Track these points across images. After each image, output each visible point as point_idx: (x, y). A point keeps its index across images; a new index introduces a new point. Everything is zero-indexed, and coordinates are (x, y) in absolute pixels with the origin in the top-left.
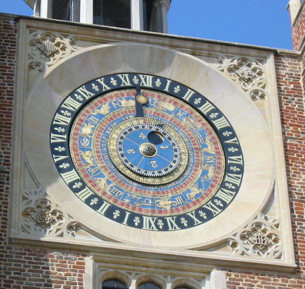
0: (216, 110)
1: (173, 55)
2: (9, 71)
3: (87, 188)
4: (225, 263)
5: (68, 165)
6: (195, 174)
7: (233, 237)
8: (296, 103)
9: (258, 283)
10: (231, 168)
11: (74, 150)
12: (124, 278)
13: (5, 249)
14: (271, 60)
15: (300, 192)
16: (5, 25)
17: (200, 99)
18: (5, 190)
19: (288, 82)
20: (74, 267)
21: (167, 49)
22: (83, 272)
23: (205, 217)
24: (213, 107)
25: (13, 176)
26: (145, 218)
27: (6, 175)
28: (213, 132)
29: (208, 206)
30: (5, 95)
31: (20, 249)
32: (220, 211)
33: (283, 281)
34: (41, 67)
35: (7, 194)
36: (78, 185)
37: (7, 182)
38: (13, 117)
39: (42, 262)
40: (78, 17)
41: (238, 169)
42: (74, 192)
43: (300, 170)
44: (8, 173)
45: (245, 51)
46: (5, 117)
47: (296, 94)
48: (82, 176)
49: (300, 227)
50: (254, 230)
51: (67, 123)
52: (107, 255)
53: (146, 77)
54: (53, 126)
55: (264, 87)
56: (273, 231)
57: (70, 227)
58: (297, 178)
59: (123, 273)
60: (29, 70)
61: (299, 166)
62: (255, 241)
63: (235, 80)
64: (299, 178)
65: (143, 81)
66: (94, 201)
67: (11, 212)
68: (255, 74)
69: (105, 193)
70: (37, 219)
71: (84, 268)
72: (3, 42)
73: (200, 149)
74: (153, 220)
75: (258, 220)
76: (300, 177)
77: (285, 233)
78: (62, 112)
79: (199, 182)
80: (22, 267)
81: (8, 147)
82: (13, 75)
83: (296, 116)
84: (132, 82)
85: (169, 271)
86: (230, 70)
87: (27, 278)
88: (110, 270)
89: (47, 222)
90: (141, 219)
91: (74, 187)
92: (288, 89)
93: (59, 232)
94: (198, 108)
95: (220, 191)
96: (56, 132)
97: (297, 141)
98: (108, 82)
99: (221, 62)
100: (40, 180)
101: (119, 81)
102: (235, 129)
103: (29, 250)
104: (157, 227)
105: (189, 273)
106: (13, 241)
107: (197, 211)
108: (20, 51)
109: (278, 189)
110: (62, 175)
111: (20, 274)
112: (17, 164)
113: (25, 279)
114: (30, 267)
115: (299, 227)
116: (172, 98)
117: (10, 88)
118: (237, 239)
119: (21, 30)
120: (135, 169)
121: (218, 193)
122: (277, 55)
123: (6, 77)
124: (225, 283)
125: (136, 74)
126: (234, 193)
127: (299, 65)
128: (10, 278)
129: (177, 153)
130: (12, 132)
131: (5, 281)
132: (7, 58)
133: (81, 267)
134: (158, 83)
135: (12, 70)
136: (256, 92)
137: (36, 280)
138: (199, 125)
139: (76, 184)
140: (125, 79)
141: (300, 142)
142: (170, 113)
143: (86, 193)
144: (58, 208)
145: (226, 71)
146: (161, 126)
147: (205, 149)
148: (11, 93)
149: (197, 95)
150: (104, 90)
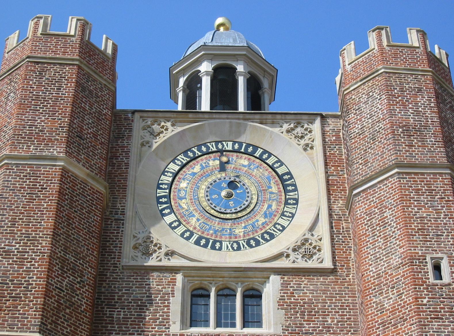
0: (279, 161)
1: (246, 125)
3: (182, 225)
4: (280, 270)
5: (169, 211)
6: (262, 208)
7: (287, 251)
8: (337, 150)
9: (305, 282)
10: (289, 201)
11: (174, 199)
12: (207, 287)
13: (119, 274)
14: (318, 121)
17: (267, 154)
21: (241, 121)
22: (175, 285)
23: (268, 238)
26: (223, 243)
27: (122, 222)
28: (277, 177)
31: (131, 273)
33: (323, 279)
34: (150, 144)
40: (200, 108)
41: (294, 202)
42: (173, 229)
43: (339, 197)
44: (123, 220)
45: (299, 117)
48: (179, 217)
50: (303, 244)
52: (193, 272)
54: (159, 184)
55: (313, 141)
56: (317, 244)
57: (167, 254)
58: (337, 203)
59: (232, 285)
65: (226, 146)
66: (187, 234)
68: (307, 132)
69: (195, 228)
71: (176, 282)
73: (267, 190)
74: (230, 243)
75: (306, 237)
76: (339, 203)
77: (326, 245)
78: (166, 174)
79: (265, 213)
80: (131, 285)
81: (124, 202)
84: (217, 147)
85: (239, 279)
86: (288, 131)
87: (134, 292)
88: (196, 282)
91: (173, 225)
92: (331, 140)
93: (159, 258)
96: (162, 189)
98: (200, 150)
99: (281, 127)
101: (208, 148)
102: (292, 173)
103: (136, 273)
104: (233, 248)
105: (254, 279)
106: (125, 267)
107: (263, 234)
108: (134, 134)
109: (321, 213)
111: (129, 290)
112: (129, 213)
113: (133, 294)
114: (136, 284)
116: (246, 156)
118: (290, 252)
119: (135, 120)
120: (217, 209)
122: (323, 117)
123: (124, 153)
124: (280, 284)
125: (221, 142)
126: (290, 219)
127: (340, 122)
128: (122, 293)
129: (249, 195)
131: (118, 296)
134: (236, 146)
136: (307, 145)
137: (140, 294)
138: (266, 174)
140: (212, 146)
141: (339, 178)
142: (245, 166)
143: (182, 229)
144: (159, 242)
145: (285, 132)
146: (238, 176)
148: (127, 165)
149: (265, 152)
150: (197, 155)
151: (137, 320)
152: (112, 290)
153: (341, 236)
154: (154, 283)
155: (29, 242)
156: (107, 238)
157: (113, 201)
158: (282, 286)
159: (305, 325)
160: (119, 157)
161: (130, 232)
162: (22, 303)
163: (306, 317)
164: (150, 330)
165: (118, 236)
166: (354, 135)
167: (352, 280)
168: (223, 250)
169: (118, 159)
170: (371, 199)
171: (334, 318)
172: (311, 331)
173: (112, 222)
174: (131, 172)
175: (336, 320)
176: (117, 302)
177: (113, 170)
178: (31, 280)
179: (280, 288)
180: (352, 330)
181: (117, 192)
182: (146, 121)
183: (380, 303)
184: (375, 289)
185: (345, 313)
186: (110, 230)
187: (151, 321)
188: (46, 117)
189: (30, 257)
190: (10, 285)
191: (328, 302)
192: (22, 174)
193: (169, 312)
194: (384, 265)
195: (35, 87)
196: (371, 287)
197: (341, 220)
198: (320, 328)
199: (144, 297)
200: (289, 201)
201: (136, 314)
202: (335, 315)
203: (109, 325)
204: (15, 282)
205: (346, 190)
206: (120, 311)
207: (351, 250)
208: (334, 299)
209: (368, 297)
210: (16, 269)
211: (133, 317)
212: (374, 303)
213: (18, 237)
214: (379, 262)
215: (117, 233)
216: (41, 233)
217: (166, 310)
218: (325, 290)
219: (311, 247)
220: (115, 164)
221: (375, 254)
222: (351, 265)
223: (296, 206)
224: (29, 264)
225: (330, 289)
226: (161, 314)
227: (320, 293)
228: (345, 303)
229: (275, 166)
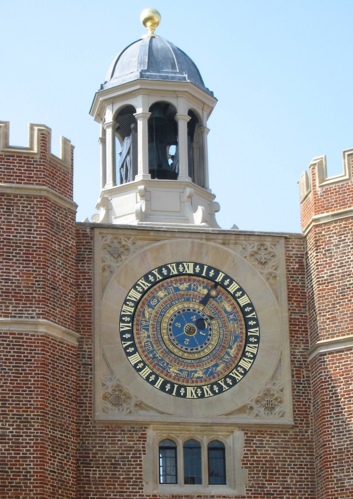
5: (133, 349)
7: (249, 403)
8: (300, 280)
9: (267, 439)
10: (251, 339)
16: (83, 234)
20: (139, 437)
21: (204, 241)
22: (145, 441)
25: (94, 368)
27: (90, 367)
30: (86, 298)
31: (102, 427)
36: (140, 366)
39: (117, 435)
43: (300, 340)
44: (91, 365)
45: (263, 238)
46: (87, 317)
52: (162, 426)
60: (103, 272)
66: (152, 378)
67: (94, 398)
71: (146, 438)
72: (83, 250)
74: (194, 389)
75: (268, 386)
76: (300, 346)
80: (104, 441)
81: (90, 343)
84: (178, 270)
85: (205, 433)
87: (108, 449)
88: (164, 435)
90: (186, 390)
92: (294, 268)
93: (129, 410)
95: (242, 360)
96: (124, 322)
98: (160, 272)
100: (113, 369)
101: (169, 271)
103: (108, 427)
104: (197, 395)
105: (219, 433)
111: (102, 447)
112: (98, 358)
113: (106, 451)
119: (96, 239)
123: (86, 281)
131: (93, 454)
133: (143, 437)
134: (198, 269)
136: (270, 274)
141: (302, 316)
145: (248, 257)
147: (229, 350)
148: (90, 296)
150: (158, 280)
151: (112, 480)
152: (86, 447)
154: (126, 439)
155: (22, 424)
158: (246, 443)
159: (267, 485)
160: (81, 285)
162: (24, 492)
163: (268, 476)
164: (125, 490)
165: (87, 384)
166: (322, 281)
167: (310, 437)
168: (188, 397)
170: (337, 365)
171: (293, 478)
172: (272, 492)
174: (97, 308)
175: (294, 480)
176: (92, 460)
178: (28, 467)
179: (245, 445)
180: (309, 490)
182: (105, 238)
183: (341, 480)
184: (336, 463)
185: (303, 473)
187: (125, 480)
188: (21, 268)
189: (24, 442)
190: (10, 473)
191: (288, 460)
192: (5, 343)
193: (141, 471)
194: (346, 441)
195: (5, 227)
196: (332, 461)
197: (302, 368)
198: (281, 489)
199: (117, 454)
200: (251, 339)
201: (111, 473)
202: (294, 475)
203: (87, 486)
204: (14, 470)
205: (307, 331)
206: (96, 471)
208: (293, 457)
209: (329, 470)
210: (13, 455)
211: (108, 476)
212: (334, 477)
213: (11, 418)
214: (341, 437)
216: (32, 414)
217: (138, 469)
218: (285, 448)
221: (338, 426)
222: (309, 419)
224: (25, 449)
225: (290, 446)
226: (134, 473)
227: (281, 451)
228: (303, 462)
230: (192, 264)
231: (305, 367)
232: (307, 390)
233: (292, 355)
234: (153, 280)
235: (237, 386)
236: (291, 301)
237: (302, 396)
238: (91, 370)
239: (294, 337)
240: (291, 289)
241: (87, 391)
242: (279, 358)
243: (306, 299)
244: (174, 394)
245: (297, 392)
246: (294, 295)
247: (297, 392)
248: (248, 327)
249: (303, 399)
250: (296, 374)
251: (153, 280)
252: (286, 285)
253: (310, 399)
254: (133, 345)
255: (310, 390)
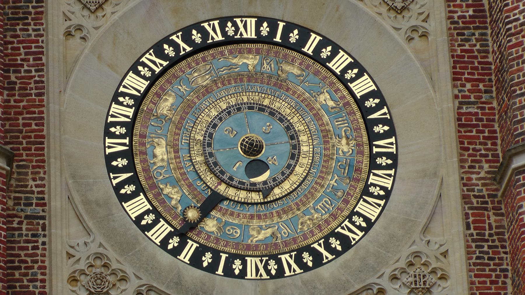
2: (35, 47)
5: (132, 188)
10: (379, 161)
15: (481, 194)
17: (329, 48)
18: (41, 247)
19: (464, 6)
24: (350, 60)
26: (249, 259)
27: (41, 222)
29: (343, 228)
30: (31, 89)
32: (361, 234)
34: (85, 33)
35: (44, 252)
36: (149, 219)
37: (43, 233)
38: (45, 125)
43: (481, 155)
44: (43, 218)
46: (34, 127)
47: (478, 24)
49: (480, 252)
50: (411, 264)
51: (128, 117)
53: (246, 21)
61: (480, 150)
62: (412, 283)
63: (380, 14)
64: (480, 170)
65: (242, 29)
70: (89, 287)
74: (261, 261)
75: (414, 248)
76: (481, 167)
81: (42, 175)
82: (42, 53)
83: (476, 64)
84: (224, 33)
89: (105, 290)
90: (244, 263)
91: (144, 222)
92: (464, 17)
94: (327, 64)
95: (361, 202)
97: (478, 108)
98: (187, 39)
104: (268, 272)
107: (326, 238)
108: (50, 12)
110: (125, 205)
112: (57, 203)
115: (477, 252)
117: (39, 76)
121: (359, 205)
123: (31, 58)
125: (231, 19)
130: (46, 150)
132: (32, 24)
134: (265, 29)
135: (40, 44)
136: (414, 29)
139: (146, 217)
141: (483, 108)
150: (183, 53)
153: (485, 244)
156: (13, 262)
157: (19, 173)
161: (59, 247)
166: (516, 27)
168: (249, 276)
169: (20, 72)
173: (21, 223)
177: (12, 99)
181: (24, 153)
186: (19, 242)
197: (486, 209)
207: (506, 277)
215: (34, 248)
219: (426, 271)
220: (15, 83)
223: (392, 172)
229: (348, 76)
230: (254, 20)
231: (494, 208)
232: (499, 253)
233: (465, 185)
234: (172, 54)
235: (351, 251)
236: (460, 79)
237: (489, 265)
238: (44, 229)
239: (467, 149)
240: (458, 56)
241: (35, 270)
242: (436, 192)
243: (491, 74)
244: (220, 271)
245: (478, 258)
246: (467, 68)
247: (478, 258)
248: (373, 137)
249: (490, 270)
250: (474, 222)
251: (172, 54)
252: (446, 48)
253: (507, 270)
254: (134, 180)
255: (506, 253)
